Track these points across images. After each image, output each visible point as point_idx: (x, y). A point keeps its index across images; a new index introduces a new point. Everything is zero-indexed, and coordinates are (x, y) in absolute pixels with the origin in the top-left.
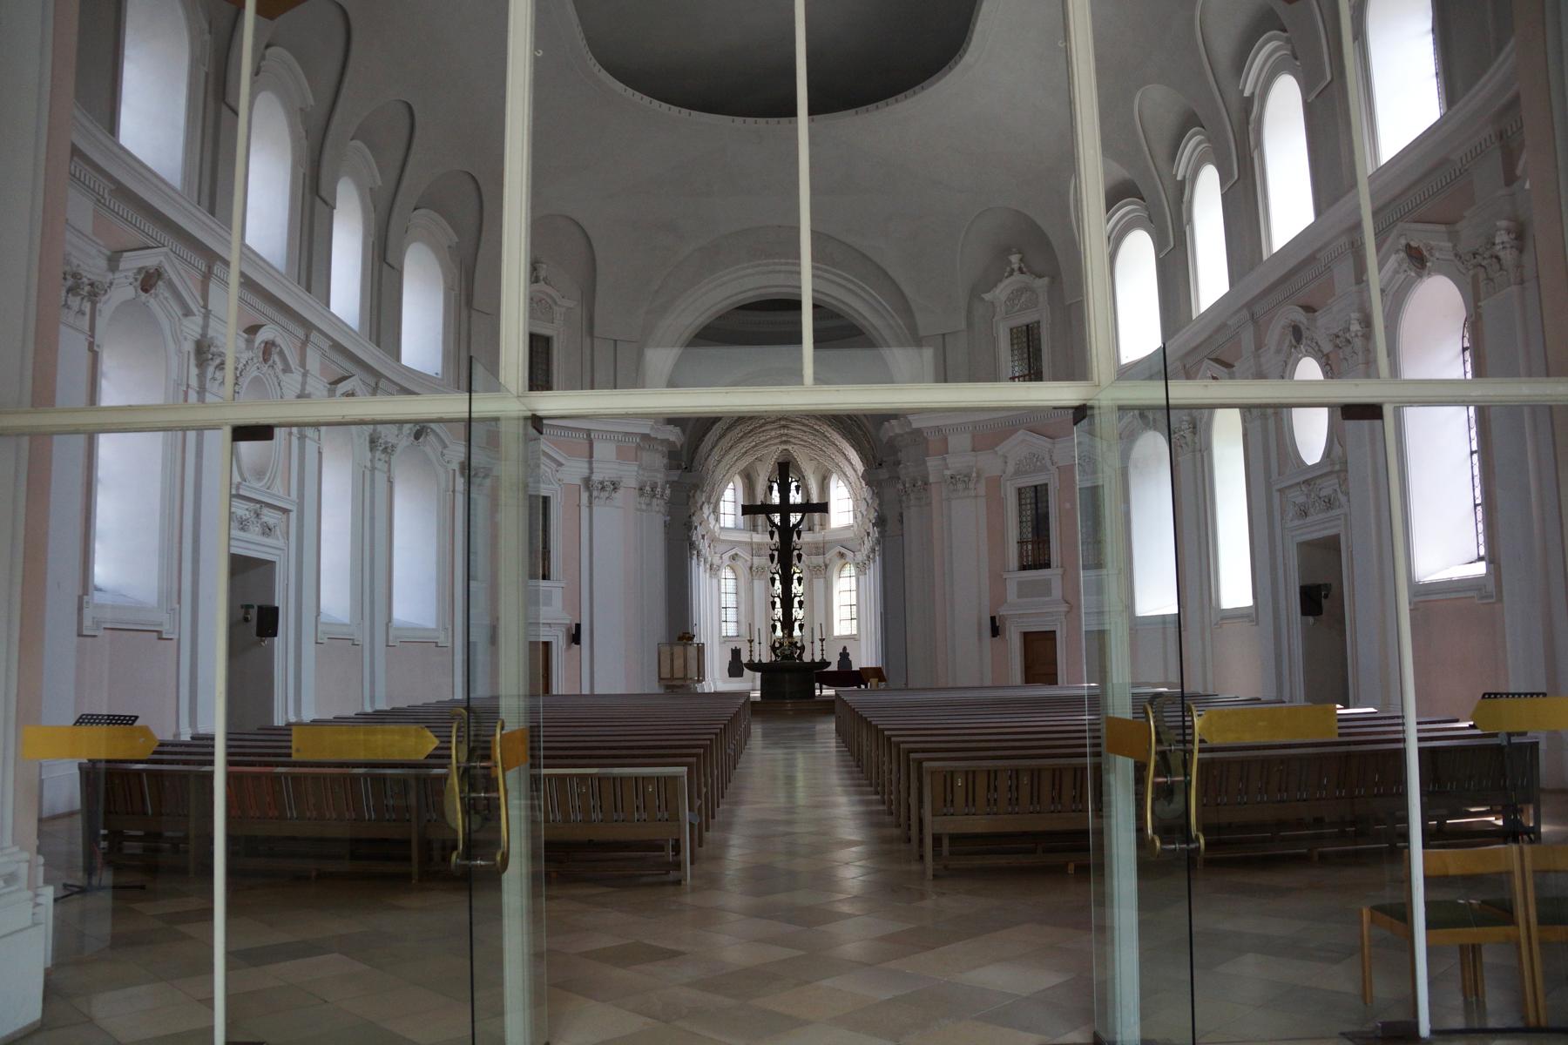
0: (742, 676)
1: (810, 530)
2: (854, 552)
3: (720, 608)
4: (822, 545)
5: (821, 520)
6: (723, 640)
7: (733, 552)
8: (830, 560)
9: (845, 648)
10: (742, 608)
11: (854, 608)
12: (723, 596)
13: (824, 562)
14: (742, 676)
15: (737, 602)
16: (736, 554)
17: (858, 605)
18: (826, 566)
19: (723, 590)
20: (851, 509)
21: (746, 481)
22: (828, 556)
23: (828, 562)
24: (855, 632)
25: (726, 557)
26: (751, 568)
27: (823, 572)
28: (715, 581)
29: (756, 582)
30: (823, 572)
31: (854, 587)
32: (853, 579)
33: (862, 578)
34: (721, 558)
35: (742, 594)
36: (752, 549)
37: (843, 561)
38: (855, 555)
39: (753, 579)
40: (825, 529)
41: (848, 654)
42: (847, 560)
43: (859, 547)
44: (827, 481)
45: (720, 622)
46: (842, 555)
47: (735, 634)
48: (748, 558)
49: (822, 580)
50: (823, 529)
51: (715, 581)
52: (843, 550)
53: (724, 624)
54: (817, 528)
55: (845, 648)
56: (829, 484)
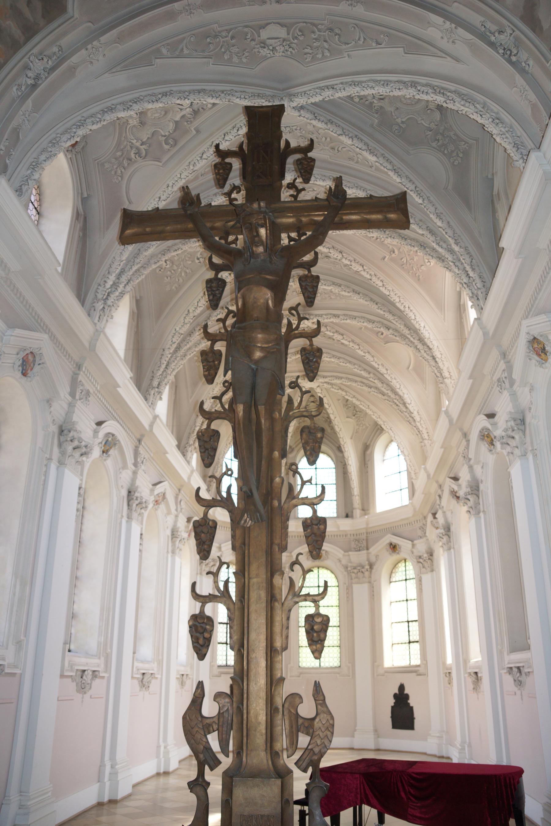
1: (347, 516)
2: (412, 541)
4: (364, 536)
5: (363, 504)
6: (216, 671)
9: (402, 688)
11: (415, 627)
13: (368, 560)
17: (421, 621)
18: (371, 566)
20: (405, 483)
22: (374, 550)
23: (373, 559)
24: (416, 661)
27: (367, 574)
30: (367, 574)
31: (413, 593)
32: (412, 585)
33: (427, 578)
38: (413, 546)
40: (369, 514)
41: (407, 697)
42: (403, 555)
43: (420, 533)
44: (368, 452)
46: (394, 547)
49: (366, 586)
50: (365, 514)
52: (396, 540)
54: (357, 512)
55: (402, 688)
56: (372, 454)
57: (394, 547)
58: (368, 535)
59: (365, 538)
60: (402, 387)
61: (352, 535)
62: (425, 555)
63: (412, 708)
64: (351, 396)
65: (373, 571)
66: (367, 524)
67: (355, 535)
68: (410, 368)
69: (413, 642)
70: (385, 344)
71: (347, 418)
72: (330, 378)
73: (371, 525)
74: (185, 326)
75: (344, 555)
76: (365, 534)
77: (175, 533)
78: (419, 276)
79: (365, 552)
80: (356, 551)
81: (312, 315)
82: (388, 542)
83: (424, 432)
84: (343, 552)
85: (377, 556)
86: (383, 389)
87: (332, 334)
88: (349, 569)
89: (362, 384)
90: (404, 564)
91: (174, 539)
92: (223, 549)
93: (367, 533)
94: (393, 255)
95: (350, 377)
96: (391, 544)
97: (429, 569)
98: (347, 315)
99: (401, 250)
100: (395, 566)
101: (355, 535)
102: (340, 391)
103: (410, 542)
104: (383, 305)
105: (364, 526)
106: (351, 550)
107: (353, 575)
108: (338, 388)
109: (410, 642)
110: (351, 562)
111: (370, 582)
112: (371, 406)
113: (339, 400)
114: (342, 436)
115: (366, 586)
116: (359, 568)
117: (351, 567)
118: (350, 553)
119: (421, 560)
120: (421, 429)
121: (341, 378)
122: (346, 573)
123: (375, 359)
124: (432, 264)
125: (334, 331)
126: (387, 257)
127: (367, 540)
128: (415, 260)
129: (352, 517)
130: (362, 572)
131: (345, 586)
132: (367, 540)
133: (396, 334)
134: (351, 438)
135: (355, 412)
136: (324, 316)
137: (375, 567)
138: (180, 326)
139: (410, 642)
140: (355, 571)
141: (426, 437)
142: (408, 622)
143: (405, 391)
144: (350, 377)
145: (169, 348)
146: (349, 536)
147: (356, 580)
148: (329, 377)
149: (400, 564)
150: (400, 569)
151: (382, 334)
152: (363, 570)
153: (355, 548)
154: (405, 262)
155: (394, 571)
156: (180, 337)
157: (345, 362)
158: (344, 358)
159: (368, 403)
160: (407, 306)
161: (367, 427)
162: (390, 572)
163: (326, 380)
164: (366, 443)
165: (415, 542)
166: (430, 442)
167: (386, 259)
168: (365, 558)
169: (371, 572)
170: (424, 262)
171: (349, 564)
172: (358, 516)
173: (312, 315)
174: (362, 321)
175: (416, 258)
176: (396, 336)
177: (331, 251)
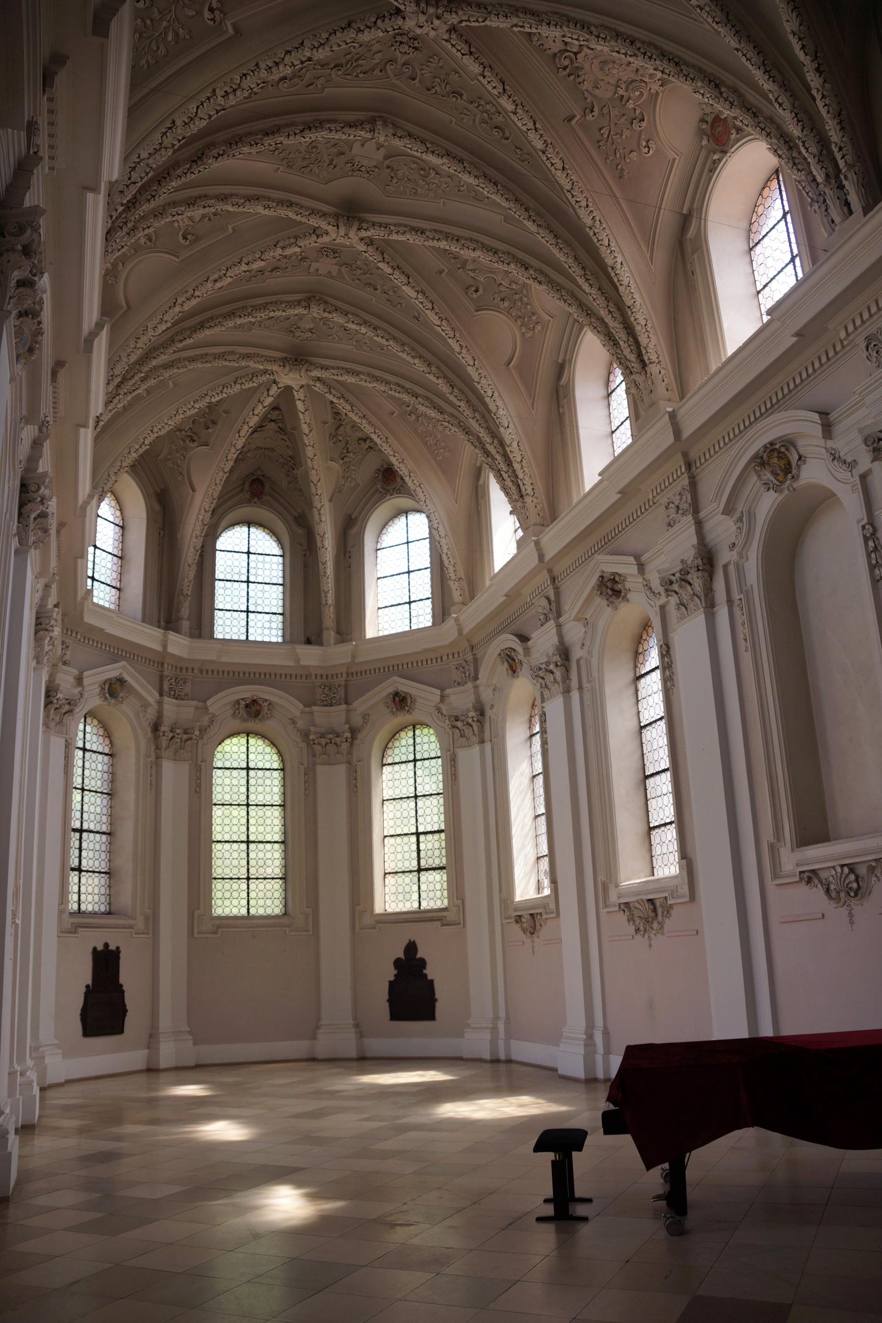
0: (121, 1031)
3: (66, 829)
4: (341, 680)
6: (68, 922)
7: (112, 671)
8: (365, 717)
9: (411, 948)
10: (127, 834)
12: (77, 796)
13: (348, 721)
14: (121, 1031)
15: (112, 818)
16: (121, 681)
18: (354, 732)
19: (77, 782)
21: (157, 507)
22: (360, 705)
23: (357, 720)
25: (94, 678)
26: (156, 727)
27: (345, 747)
28: (57, 743)
29: (168, 766)
30: (345, 747)
34: (79, 680)
35: (129, 795)
36: (161, 678)
37: (402, 718)
39: (158, 757)
41: (423, 963)
42: (416, 716)
44: (353, 531)
45: (65, 869)
46: (400, 701)
47: (103, 909)
48: (151, 696)
49: (342, 769)
51: (57, 743)
52: (405, 686)
53: (74, 877)
55: (411, 948)
57: (400, 701)
58: (350, 678)
59: (343, 683)
60: (496, 394)
61: (319, 677)
62: (472, 714)
63: (432, 981)
64: (360, 415)
65: (357, 742)
66: (353, 657)
67: (324, 677)
68: (512, 365)
69: (427, 870)
70: (476, 311)
71: (331, 460)
72: (335, 372)
73: (359, 660)
74: (163, 152)
75: (302, 712)
76: (344, 675)
77: (43, 620)
78: (622, 169)
79: (343, 707)
80: (324, 705)
81: (367, 222)
82: (391, 690)
83: (527, 481)
84: (302, 706)
85: (365, 717)
86: (452, 398)
87: (389, 271)
88: (312, 737)
89: (398, 389)
90: (411, 734)
91: (41, 633)
92: (86, 682)
93: (348, 674)
94: (589, 117)
95: (377, 373)
96: (396, 694)
97: (475, 739)
98: (441, 232)
99: (605, 111)
100: (394, 735)
101: (324, 677)
102: (342, 401)
103: (438, 692)
104: (538, 214)
105: (349, 660)
106: (315, 705)
107: (318, 748)
108: (340, 395)
109: (420, 870)
110: (315, 725)
111: (349, 763)
112: (391, 440)
113: (325, 423)
114: (319, 492)
115: (341, 770)
116: (331, 736)
117: (316, 733)
118: (315, 708)
119: (459, 724)
120: (521, 476)
121: (358, 374)
122: (304, 745)
123: (457, 335)
124: (651, 152)
125: (395, 265)
126: (578, 117)
127: (346, 686)
128: (624, 137)
129: (320, 643)
130: (335, 744)
131: (302, 767)
132: (346, 686)
133: (540, 278)
134: (330, 501)
135: (345, 451)
136: (392, 228)
137: (360, 736)
138: (152, 151)
139: (420, 870)
140: (323, 741)
141: (530, 491)
142: (418, 834)
143: (500, 403)
144: (377, 373)
145: (122, 192)
146: (313, 677)
147: (324, 757)
148: (333, 368)
149: (403, 734)
150: (403, 742)
151: (476, 291)
152: (338, 740)
153: (323, 701)
154: (605, 136)
155: (390, 745)
156: (147, 174)
157: (387, 337)
158: (385, 331)
159: (389, 435)
160: (597, 218)
161: (358, 485)
162: (384, 746)
163: (323, 374)
164: (350, 516)
165: (448, 691)
166: (535, 500)
167: (574, 122)
168: (343, 718)
169: (352, 743)
170: (639, 144)
171: (312, 729)
172: (332, 641)
173: (367, 222)
174: (472, 246)
175: (626, 133)
176: (540, 283)
177: (486, 73)
